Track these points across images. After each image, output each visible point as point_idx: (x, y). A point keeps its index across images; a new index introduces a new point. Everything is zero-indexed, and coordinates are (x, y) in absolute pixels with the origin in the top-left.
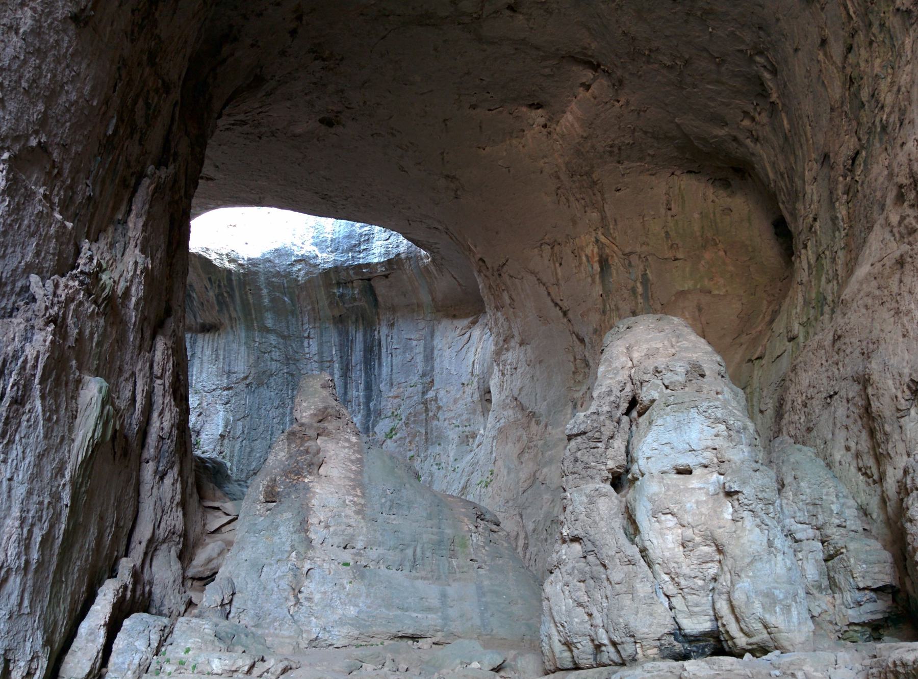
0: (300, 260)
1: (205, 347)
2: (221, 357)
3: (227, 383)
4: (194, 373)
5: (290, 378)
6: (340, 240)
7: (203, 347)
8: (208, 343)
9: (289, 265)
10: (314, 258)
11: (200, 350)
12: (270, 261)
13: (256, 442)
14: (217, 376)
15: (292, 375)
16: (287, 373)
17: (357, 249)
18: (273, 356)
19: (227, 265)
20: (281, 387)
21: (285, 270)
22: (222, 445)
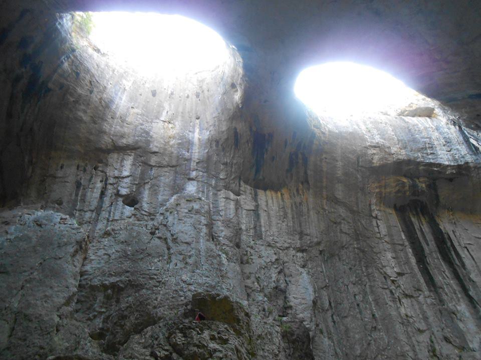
0: (375, 147)
1: (270, 202)
2: (290, 216)
3: (301, 244)
4: (262, 224)
5: (361, 255)
6: (406, 142)
7: (267, 202)
8: (272, 199)
9: (365, 147)
10: (388, 148)
11: (265, 203)
12: (347, 139)
13: (347, 319)
14: (288, 234)
15: (363, 251)
16: (357, 248)
17: (425, 152)
18: (342, 228)
19: (313, 128)
20: (353, 262)
21: (361, 151)
22: (315, 316)
